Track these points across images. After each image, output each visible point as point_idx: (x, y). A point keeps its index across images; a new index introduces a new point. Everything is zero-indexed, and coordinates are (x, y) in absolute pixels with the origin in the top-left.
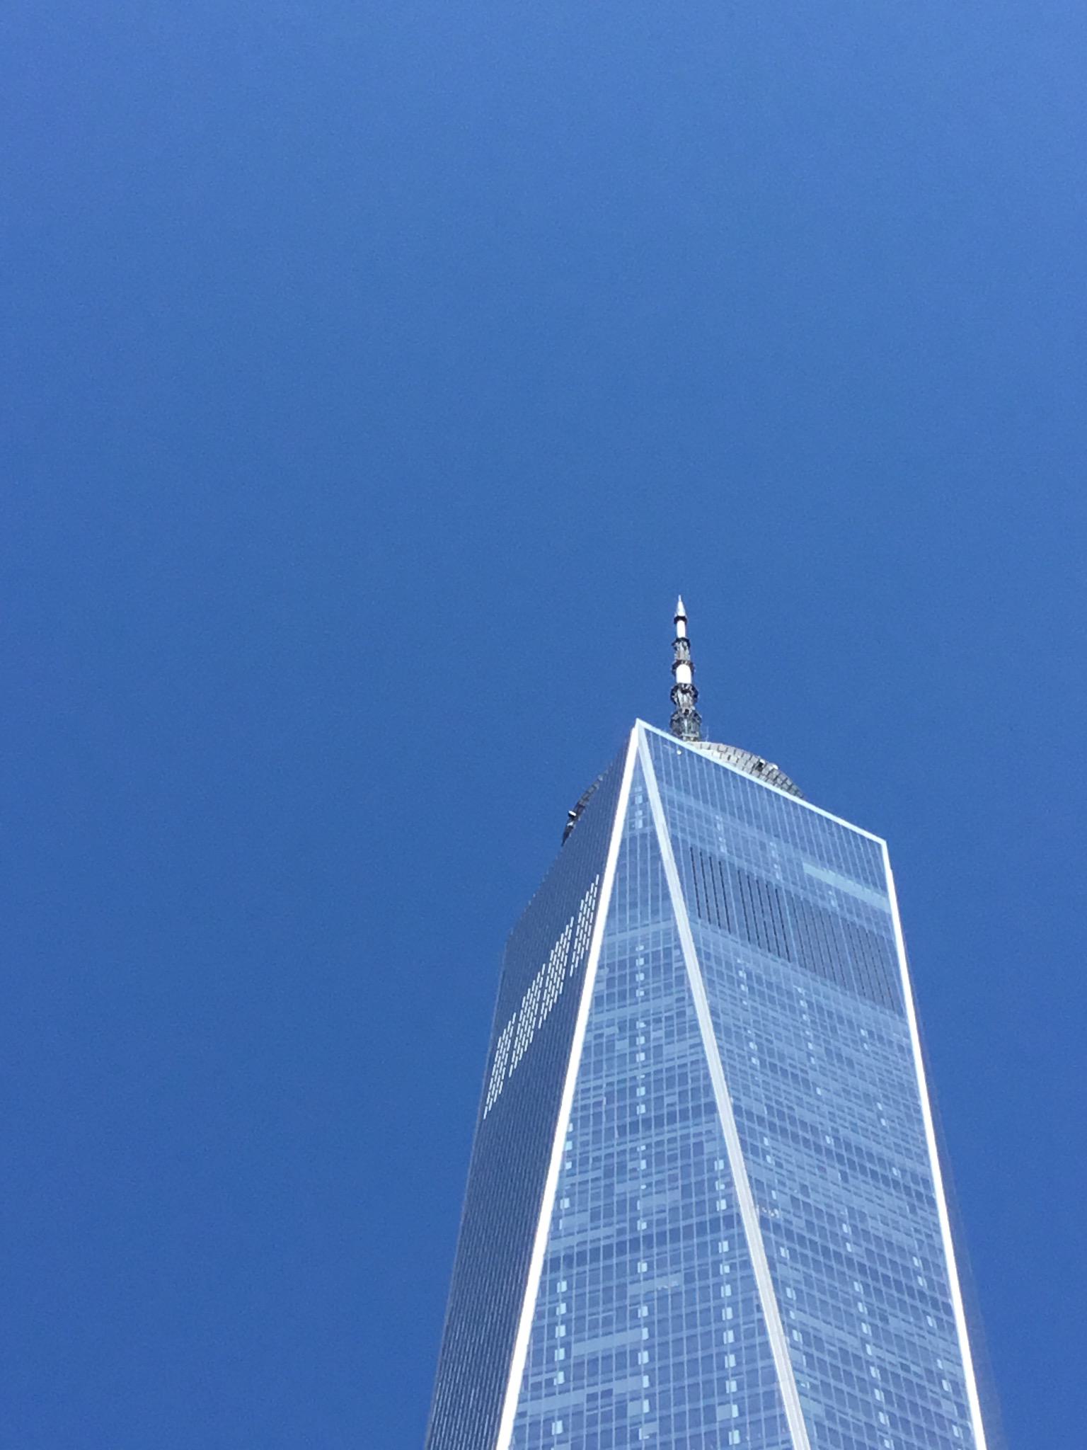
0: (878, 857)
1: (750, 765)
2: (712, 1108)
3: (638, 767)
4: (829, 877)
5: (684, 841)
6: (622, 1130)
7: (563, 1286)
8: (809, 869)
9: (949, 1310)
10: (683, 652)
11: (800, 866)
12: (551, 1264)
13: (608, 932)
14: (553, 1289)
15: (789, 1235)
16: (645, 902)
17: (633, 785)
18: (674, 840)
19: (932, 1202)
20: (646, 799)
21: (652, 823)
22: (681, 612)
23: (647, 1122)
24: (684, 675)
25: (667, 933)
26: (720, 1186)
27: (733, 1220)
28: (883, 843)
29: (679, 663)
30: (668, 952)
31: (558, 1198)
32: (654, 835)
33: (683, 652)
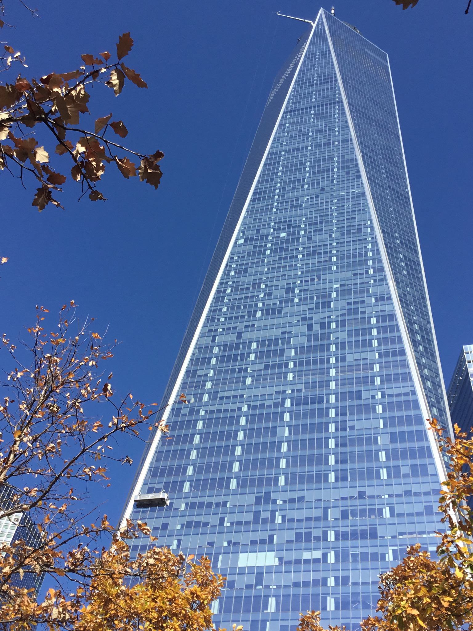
2: (336, 80)
3: (321, 15)
4: (372, 54)
6: (309, 86)
9: (399, 137)
12: (286, 112)
14: (286, 116)
15: (356, 108)
16: (320, 42)
17: (319, 19)
19: (396, 118)
20: (322, 22)
21: (324, 26)
22: (333, 7)
23: (316, 84)
25: (326, 48)
26: (337, 96)
27: (340, 102)
32: (324, 29)
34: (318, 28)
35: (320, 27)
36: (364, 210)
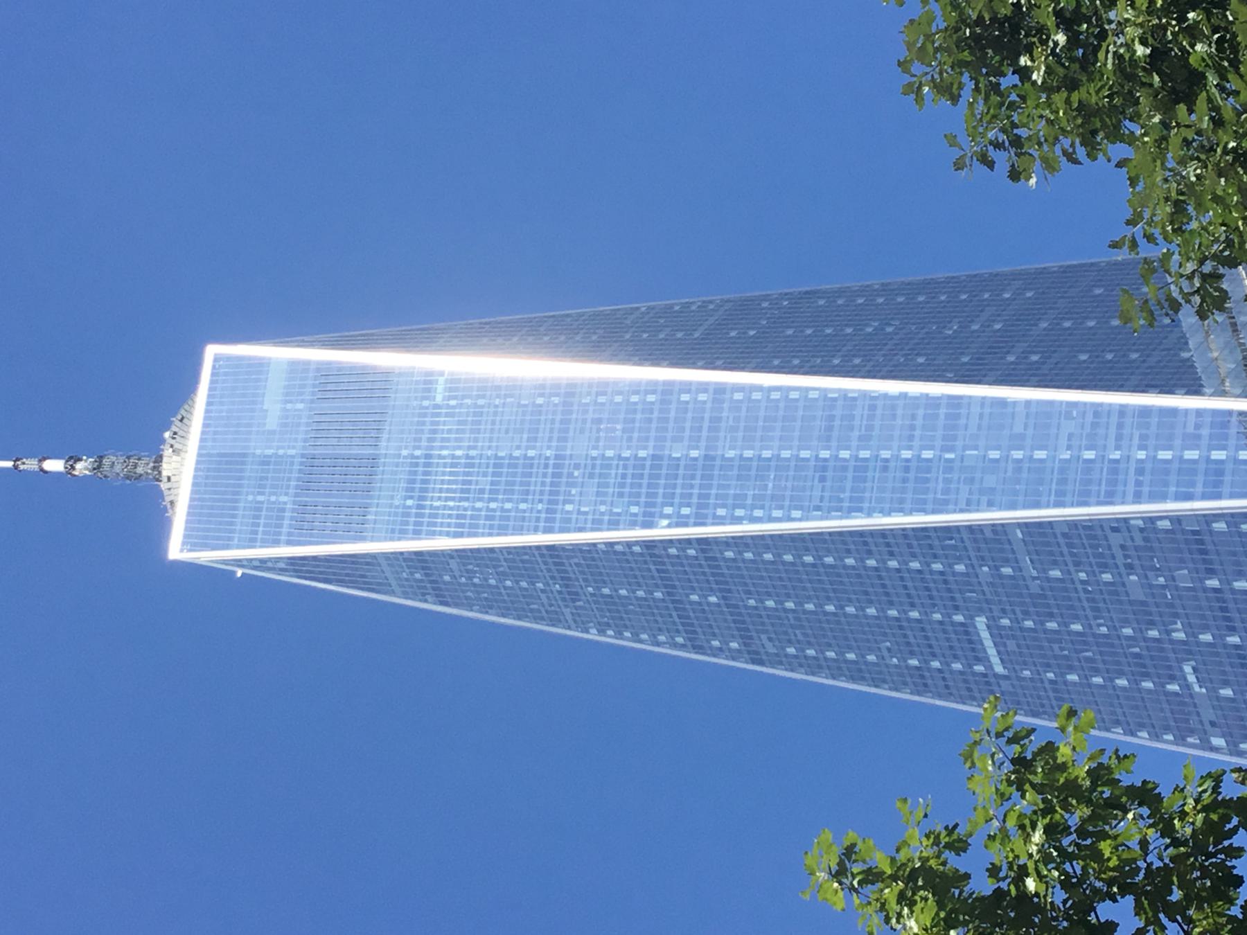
0: (229, 358)
1: (175, 458)
5: (289, 534)
7: (716, 643)
8: (272, 423)
10: (30, 465)
11: (273, 432)
12: (698, 649)
13: (393, 593)
18: (290, 543)
24: (55, 465)
28: (212, 351)
29: (42, 470)
30: (405, 560)
31: (641, 641)
33: (30, 465)
34: (281, 570)
35: (282, 565)
36: (1085, 528)
